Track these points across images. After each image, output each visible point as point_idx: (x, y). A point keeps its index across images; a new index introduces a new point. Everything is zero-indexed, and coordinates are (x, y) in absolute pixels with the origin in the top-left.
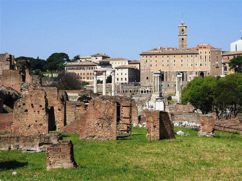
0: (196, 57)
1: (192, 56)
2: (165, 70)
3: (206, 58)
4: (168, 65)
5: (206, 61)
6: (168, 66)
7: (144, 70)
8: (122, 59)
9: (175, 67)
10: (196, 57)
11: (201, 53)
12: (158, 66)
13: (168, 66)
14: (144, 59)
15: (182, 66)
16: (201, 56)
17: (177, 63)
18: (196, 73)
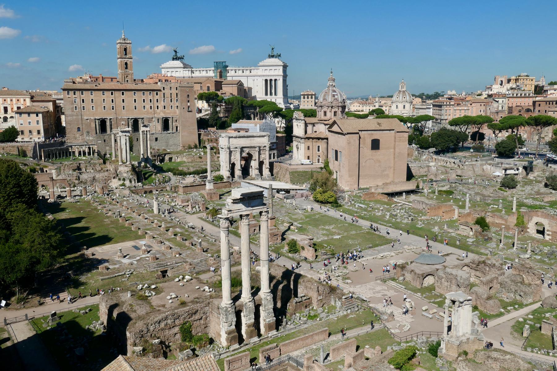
0: (157, 94)
1: (150, 93)
2: (108, 115)
3: (171, 97)
5: (171, 102)
6: (113, 109)
7: (72, 115)
8: (17, 93)
9: (124, 112)
10: (157, 94)
11: (164, 89)
12: (96, 108)
13: (113, 109)
14: (70, 96)
15: (135, 109)
16: (164, 94)
18: (158, 120)
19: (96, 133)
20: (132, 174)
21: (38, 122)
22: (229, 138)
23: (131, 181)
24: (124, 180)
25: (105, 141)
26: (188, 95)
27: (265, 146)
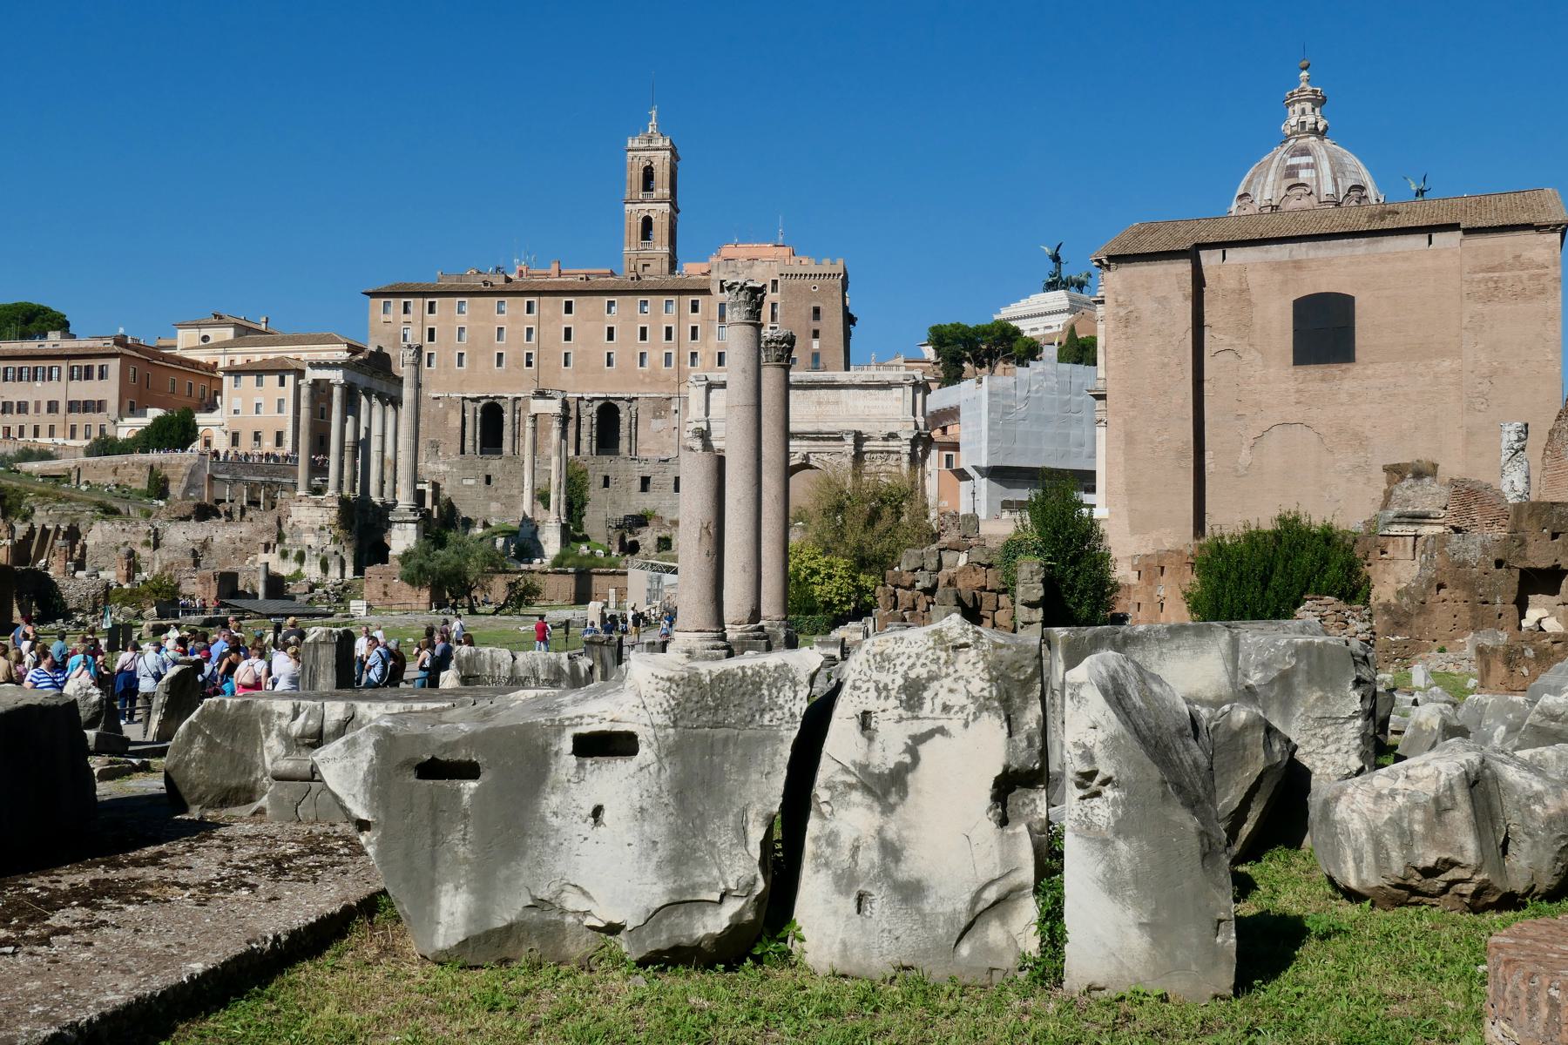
0: (695, 309)
2: (507, 387)
4: (529, 355)
6: (529, 364)
10: (695, 309)
12: (470, 361)
13: (529, 364)
14: (390, 318)
15: (609, 363)
17: (580, 348)
19: (463, 452)
20: (336, 540)
21: (281, 401)
22: (710, 387)
23: (325, 567)
24: (301, 558)
25: (488, 480)
26: (817, 311)
27: (892, 436)
